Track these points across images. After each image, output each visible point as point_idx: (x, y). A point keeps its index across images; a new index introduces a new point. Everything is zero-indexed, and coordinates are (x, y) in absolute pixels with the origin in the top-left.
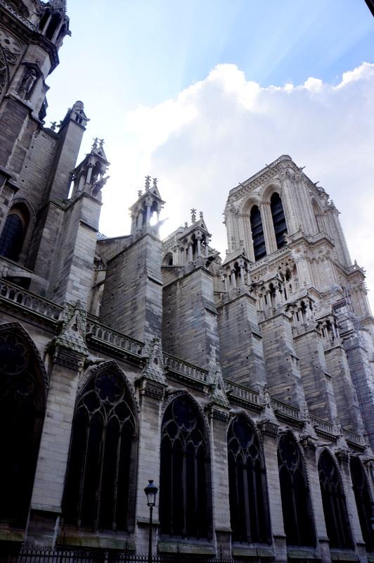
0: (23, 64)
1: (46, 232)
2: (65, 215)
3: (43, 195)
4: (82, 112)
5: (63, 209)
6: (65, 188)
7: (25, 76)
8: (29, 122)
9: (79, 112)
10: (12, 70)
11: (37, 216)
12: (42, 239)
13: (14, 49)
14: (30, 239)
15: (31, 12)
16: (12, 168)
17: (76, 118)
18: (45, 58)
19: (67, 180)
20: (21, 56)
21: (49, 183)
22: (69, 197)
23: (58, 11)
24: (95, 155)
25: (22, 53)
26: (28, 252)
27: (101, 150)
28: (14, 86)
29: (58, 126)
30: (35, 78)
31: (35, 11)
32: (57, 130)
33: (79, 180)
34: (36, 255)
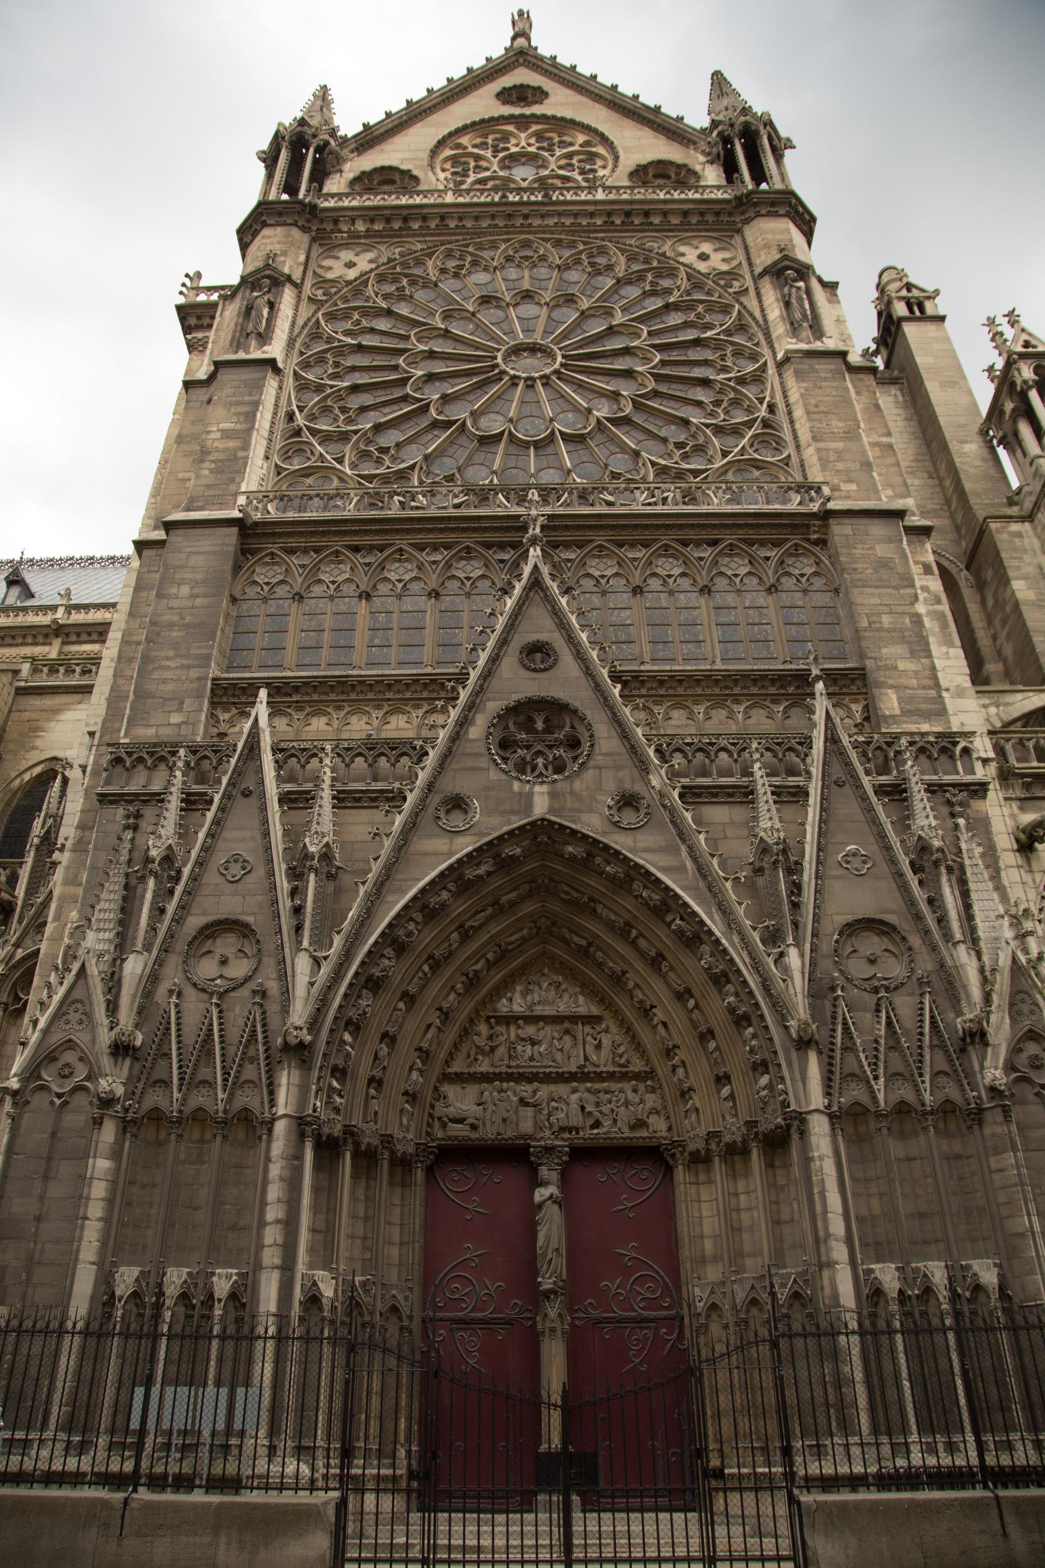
0: (761, 275)
1: (1020, 588)
2: (1035, 529)
3: (952, 516)
4: (909, 287)
5: (1022, 519)
6: (992, 471)
7: (783, 296)
8: (852, 381)
9: (904, 293)
10: (752, 304)
11: (968, 568)
12: (1022, 607)
13: (724, 260)
14: (985, 624)
15: (698, 168)
16: (890, 492)
17: (903, 310)
18: (788, 231)
19: (985, 452)
20: (745, 264)
21: (947, 483)
22: (1015, 484)
23: (742, 119)
24: (1023, 356)
25: (741, 257)
26: (999, 652)
27: (1025, 337)
28: (779, 329)
29: (876, 352)
30: (801, 284)
31: (702, 158)
32: (879, 362)
33: (1016, 434)
34: (1033, 649)
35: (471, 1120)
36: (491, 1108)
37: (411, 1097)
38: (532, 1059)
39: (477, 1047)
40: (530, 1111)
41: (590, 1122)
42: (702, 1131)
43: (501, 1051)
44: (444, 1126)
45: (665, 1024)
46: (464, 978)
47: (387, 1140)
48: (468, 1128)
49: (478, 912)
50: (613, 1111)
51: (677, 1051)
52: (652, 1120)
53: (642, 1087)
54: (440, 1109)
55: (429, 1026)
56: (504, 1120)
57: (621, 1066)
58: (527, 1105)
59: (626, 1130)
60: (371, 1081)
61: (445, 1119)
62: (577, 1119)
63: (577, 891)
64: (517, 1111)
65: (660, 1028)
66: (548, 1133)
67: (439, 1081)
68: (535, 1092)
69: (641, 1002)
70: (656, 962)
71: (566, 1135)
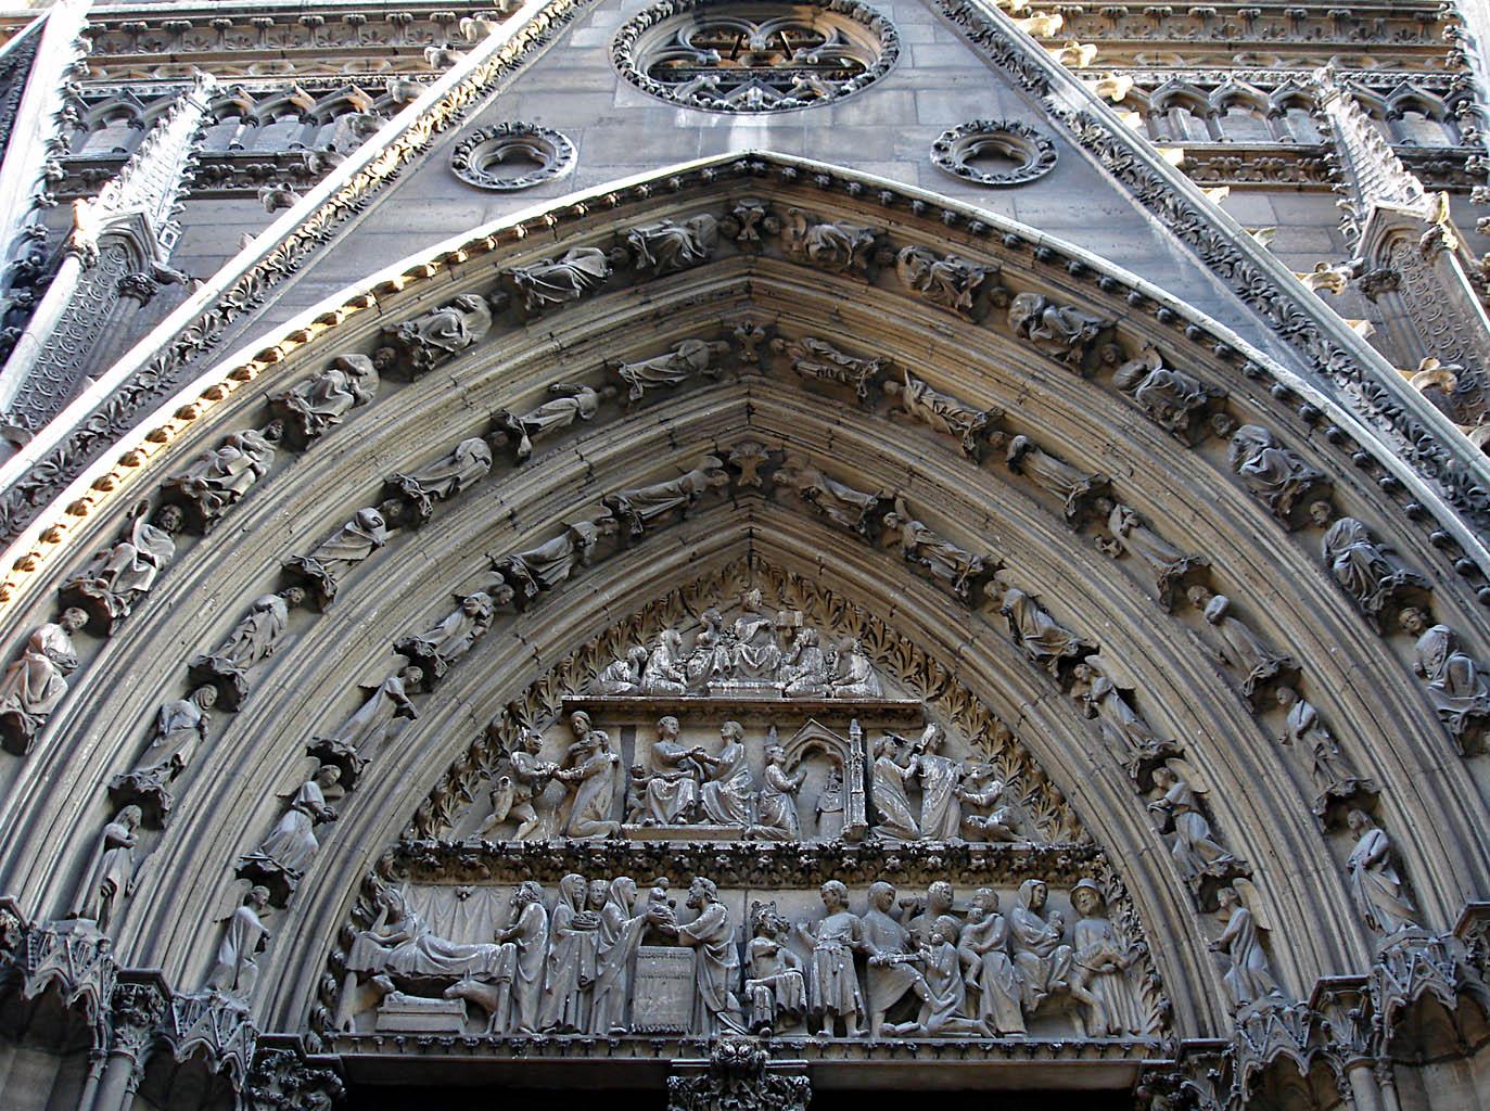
35: (465, 986)
36: (540, 947)
37: (268, 882)
38: (695, 812)
39: (521, 779)
40: (676, 960)
41: (888, 996)
42: (1297, 993)
43: (600, 792)
44: (380, 996)
45: (1127, 696)
46: (497, 578)
47: (139, 990)
48: (461, 1007)
49: (551, 394)
50: (964, 966)
51: (1178, 767)
52: (1103, 992)
53: (1059, 899)
54: (370, 950)
55: (369, 693)
56: (587, 988)
57: (987, 835)
58: (672, 939)
59: (1011, 1023)
60: (122, 795)
61: (383, 980)
62: (838, 987)
63: (844, 351)
64: (632, 960)
65: (1114, 704)
66: (736, 1029)
67: (380, 867)
68: (696, 906)
69: (1047, 639)
70: (1090, 508)
71: (803, 1037)
